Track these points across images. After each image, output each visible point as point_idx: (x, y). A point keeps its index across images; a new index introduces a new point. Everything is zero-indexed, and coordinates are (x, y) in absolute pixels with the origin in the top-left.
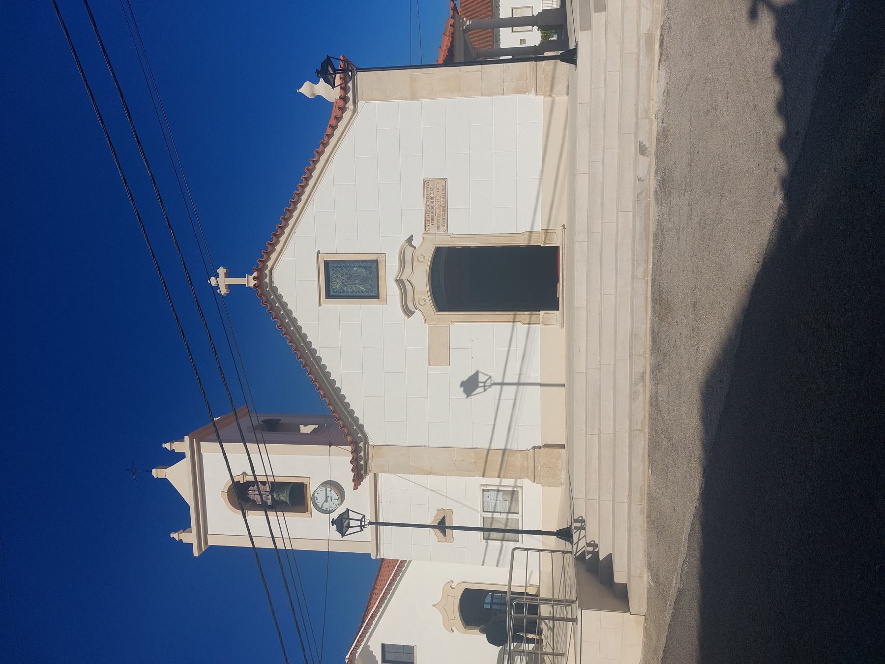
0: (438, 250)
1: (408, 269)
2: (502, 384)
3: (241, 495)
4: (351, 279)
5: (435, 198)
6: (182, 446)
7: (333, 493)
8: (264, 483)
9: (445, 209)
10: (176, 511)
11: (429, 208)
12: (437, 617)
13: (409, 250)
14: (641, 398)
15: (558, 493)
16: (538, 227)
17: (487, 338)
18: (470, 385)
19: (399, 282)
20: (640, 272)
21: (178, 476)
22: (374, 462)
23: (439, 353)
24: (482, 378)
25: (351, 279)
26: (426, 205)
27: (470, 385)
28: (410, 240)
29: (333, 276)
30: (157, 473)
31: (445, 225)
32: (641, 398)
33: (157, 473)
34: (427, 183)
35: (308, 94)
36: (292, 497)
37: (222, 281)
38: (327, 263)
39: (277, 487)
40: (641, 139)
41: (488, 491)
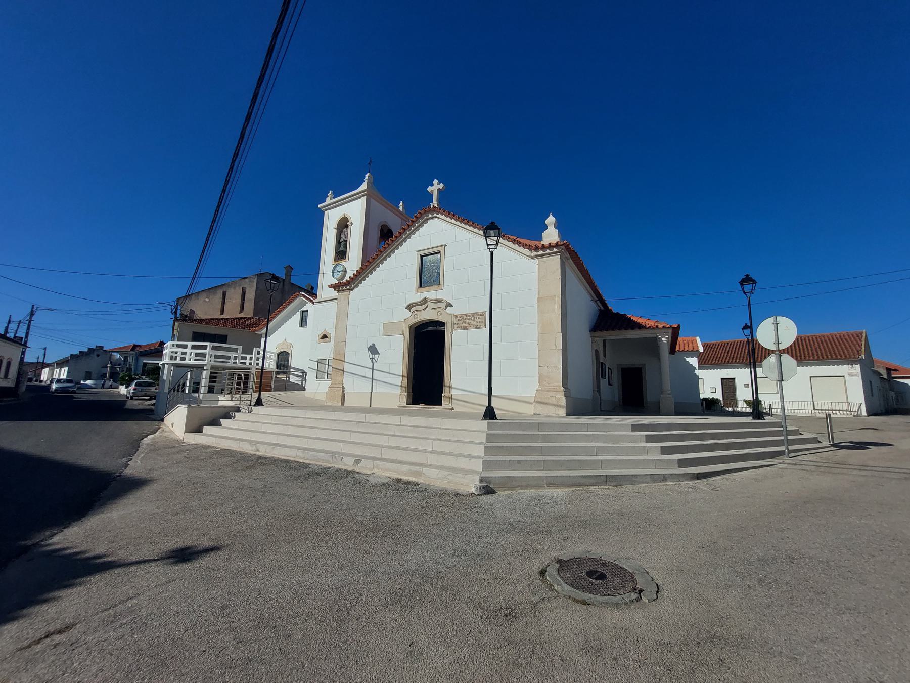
0: (443, 324)
3: (343, 225)
9: (467, 328)
11: (469, 316)
13: (443, 305)
17: (396, 356)
18: (373, 350)
19: (425, 301)
23: (389, 329)
24: (376, 356)
27: (373, 350)
28: (451, 305)
31: (458, 329)
35: (547, 221)
36: (341, 254)
37: (436, 187)
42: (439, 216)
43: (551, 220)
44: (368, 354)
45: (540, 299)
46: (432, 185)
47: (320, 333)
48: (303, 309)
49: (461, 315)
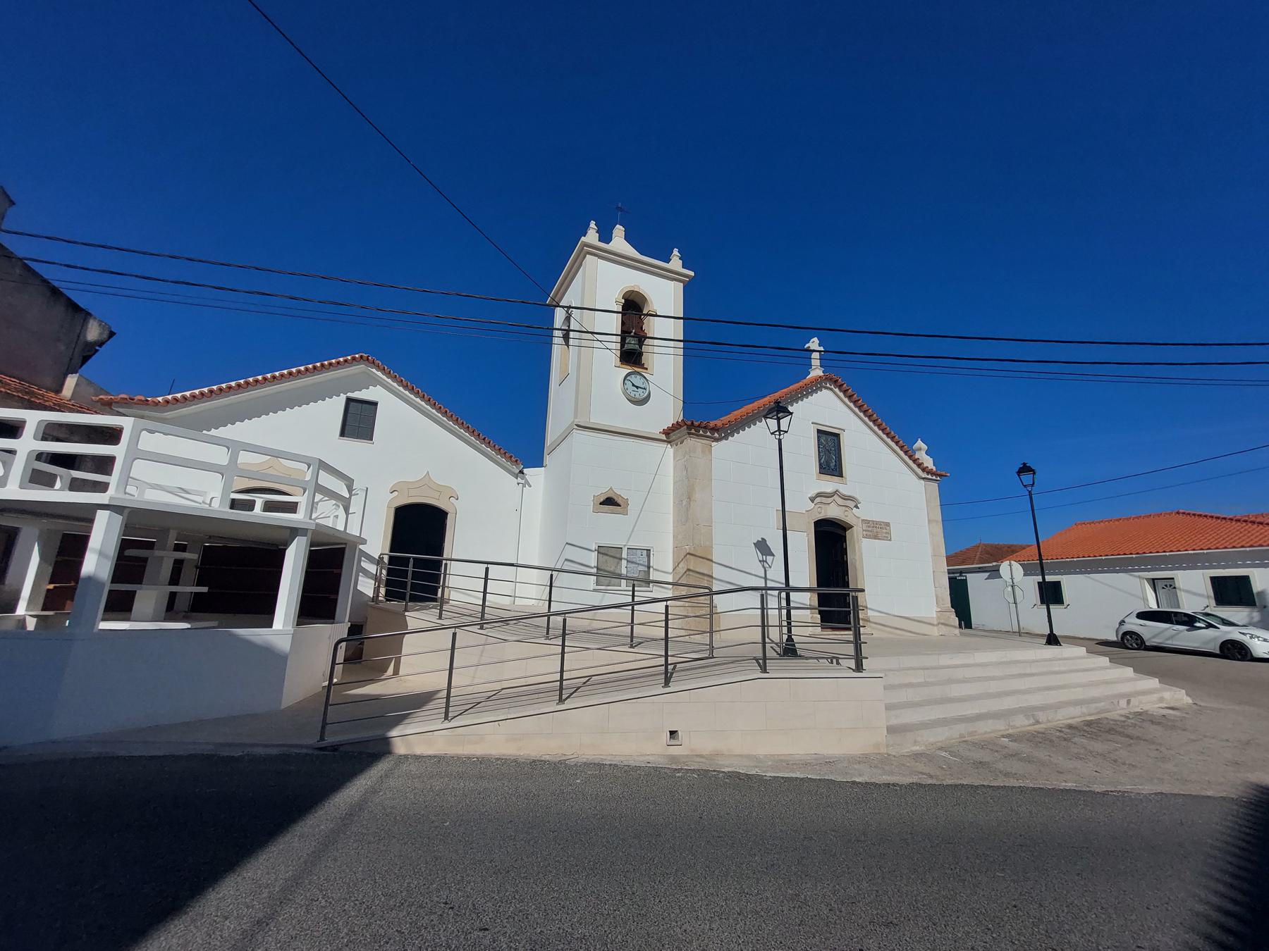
1: (840, 501)
4: (830, 453)
5: (879, 530)
6: (676, 263)
7: (640, 394)
9: (876, 537)
12: (413, 477)
14: (1026, 722)
16: (870, 613)
19: (836, 492)
24: (769, 559)
25: (830, 453)
26: (877, 523)
29: (830, 438)
31: (867, 537)
34: (888, 524)
35: (915, 446)
38: (837, 436)
39: (642, 338)
41: (649, 556)
42: (837, 390)
44: (755, 555)
47: (602, 491)
48: (350, 395)
49: (868, 522)
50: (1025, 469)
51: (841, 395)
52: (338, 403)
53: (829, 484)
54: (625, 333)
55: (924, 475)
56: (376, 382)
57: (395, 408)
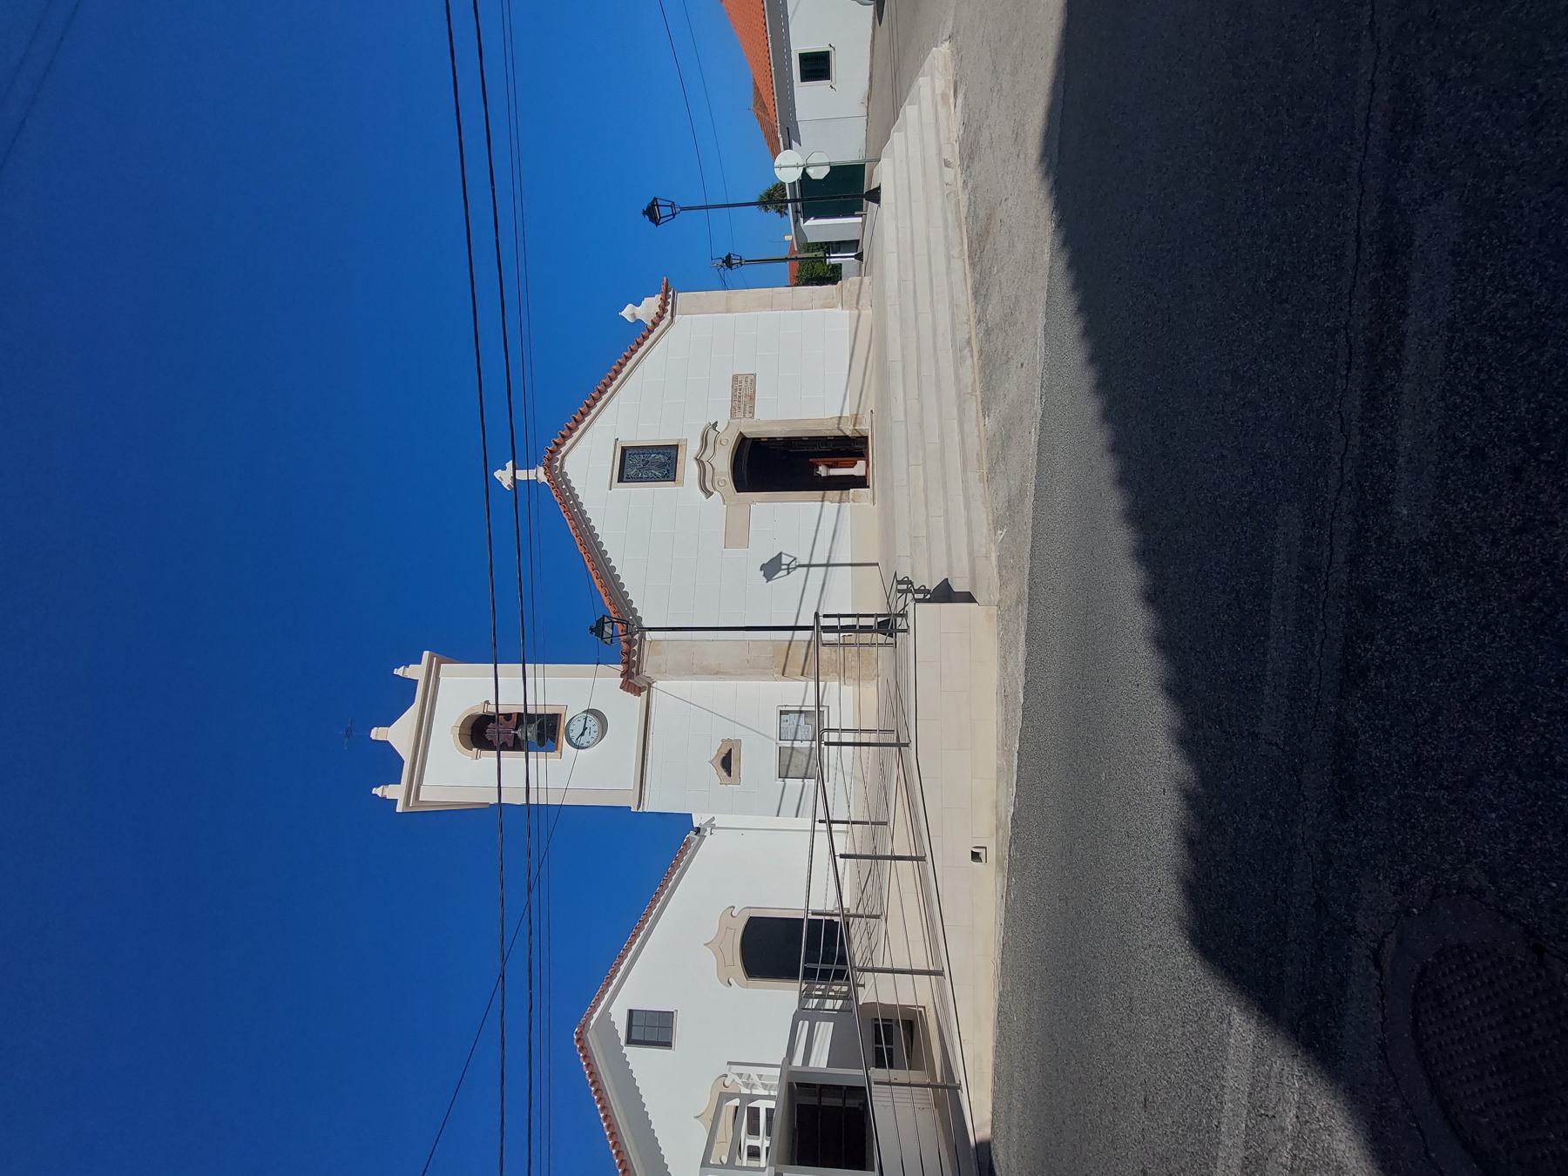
1: (709, 452)
2: (809, 566)
4: (648, 464)
5: (743, 392)
6: (416, 672)
7: (593, 723)
8: (508, 716)
9: (752, 398)
10: (387, 764)
12: (710, 959)
13: (712, 432)
14: (969, 362)
15: (870, 691)
17: (787, 517)
18: (771, 569)
20: (955, 252)
21: (399, 734)
22: (648, 669)
23: (736, 536)
24: (785, 560)
25: (648, 464)
27: (771, 569)
29: (627, 461)
30: (377, 734)
31: (752, 412)
32: (969, 362)
33: (377, 734)
34: (735, 378)
35: (630, 319)
36: (542, 731)
38: (624, 450)
39: (523, 719)
40: (945, 156)
41: (787, 712)
42: (564, 449)
43: (627, 312)
44: (781, 581)
45: (728, 311)
46: (504, 468)
47: (714, 773)
48: (622, 1035)
50: (651, 212)
51: (569, 442)
52: (634, 1055)
53: (688, 468)
54: (517, 745)
55: (668, 316)
56: (606, 1013)
57: (637, 987)
